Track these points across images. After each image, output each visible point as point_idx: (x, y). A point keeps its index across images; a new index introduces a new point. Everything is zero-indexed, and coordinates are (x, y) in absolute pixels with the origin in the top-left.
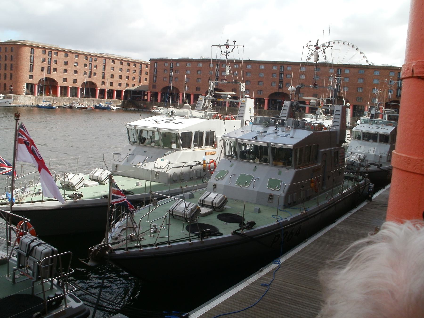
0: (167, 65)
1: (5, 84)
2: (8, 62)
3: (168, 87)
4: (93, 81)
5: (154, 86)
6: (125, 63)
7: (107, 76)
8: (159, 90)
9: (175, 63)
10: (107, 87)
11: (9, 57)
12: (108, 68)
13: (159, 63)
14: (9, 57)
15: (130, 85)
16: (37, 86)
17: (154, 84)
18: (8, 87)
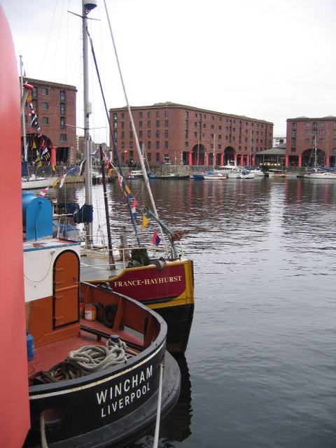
0: (308, 125)
1: (158, 154)
2: (162, 129)
3: (311, 150)
4: (232, 146)
5: (293, 149)
6: (250, 123)
7: (243, 139)
8: (299, 153)
9: (318, 122)
10: (243, 152)
11: (162, 122)
12: (243, 131)
13: (299, 123)
14: (162, 122)
15: (259, 149)
16: (191, 155)
17: (294, 146)
18: (162, 158)
